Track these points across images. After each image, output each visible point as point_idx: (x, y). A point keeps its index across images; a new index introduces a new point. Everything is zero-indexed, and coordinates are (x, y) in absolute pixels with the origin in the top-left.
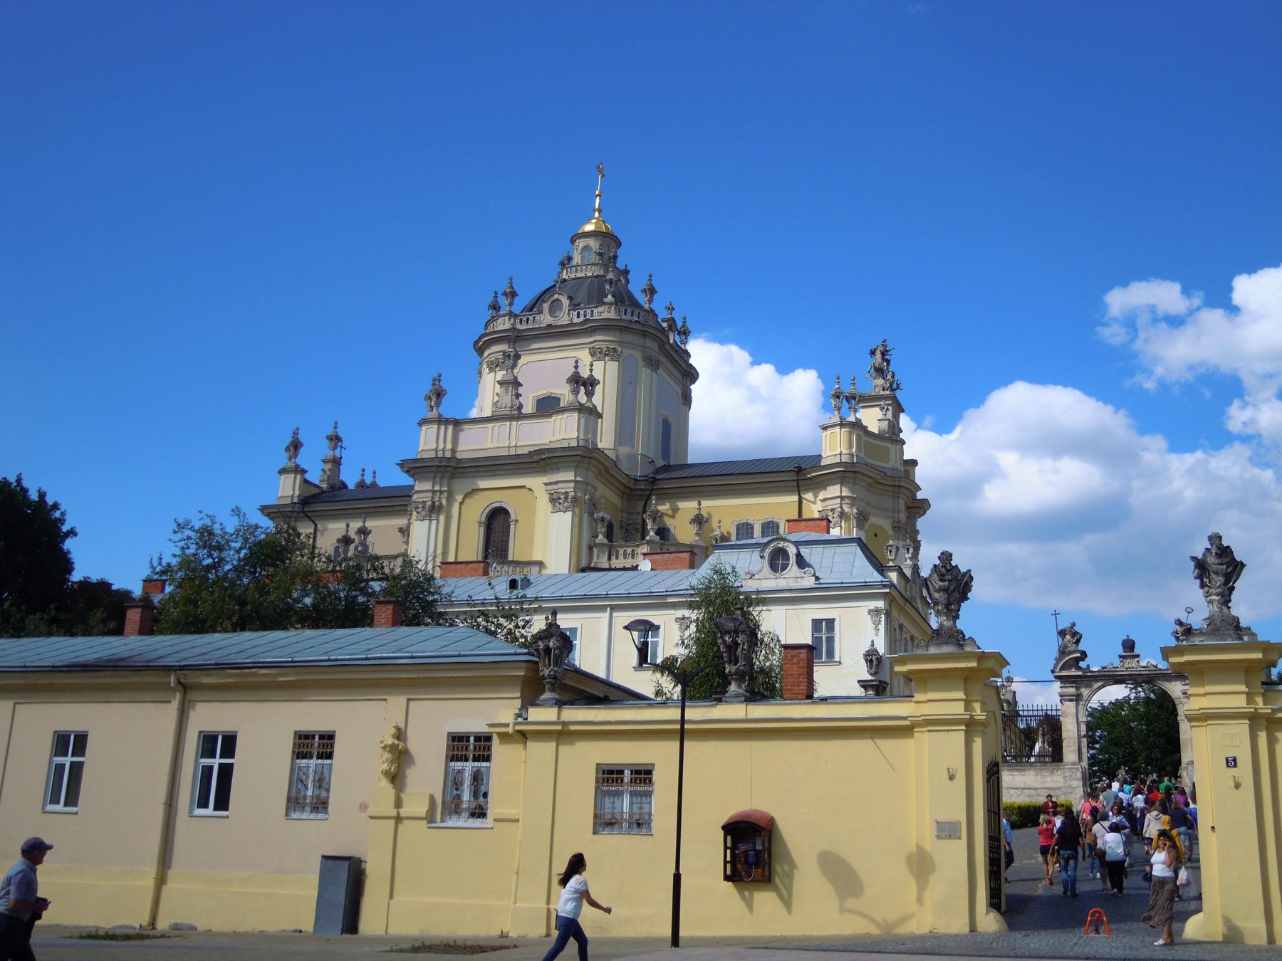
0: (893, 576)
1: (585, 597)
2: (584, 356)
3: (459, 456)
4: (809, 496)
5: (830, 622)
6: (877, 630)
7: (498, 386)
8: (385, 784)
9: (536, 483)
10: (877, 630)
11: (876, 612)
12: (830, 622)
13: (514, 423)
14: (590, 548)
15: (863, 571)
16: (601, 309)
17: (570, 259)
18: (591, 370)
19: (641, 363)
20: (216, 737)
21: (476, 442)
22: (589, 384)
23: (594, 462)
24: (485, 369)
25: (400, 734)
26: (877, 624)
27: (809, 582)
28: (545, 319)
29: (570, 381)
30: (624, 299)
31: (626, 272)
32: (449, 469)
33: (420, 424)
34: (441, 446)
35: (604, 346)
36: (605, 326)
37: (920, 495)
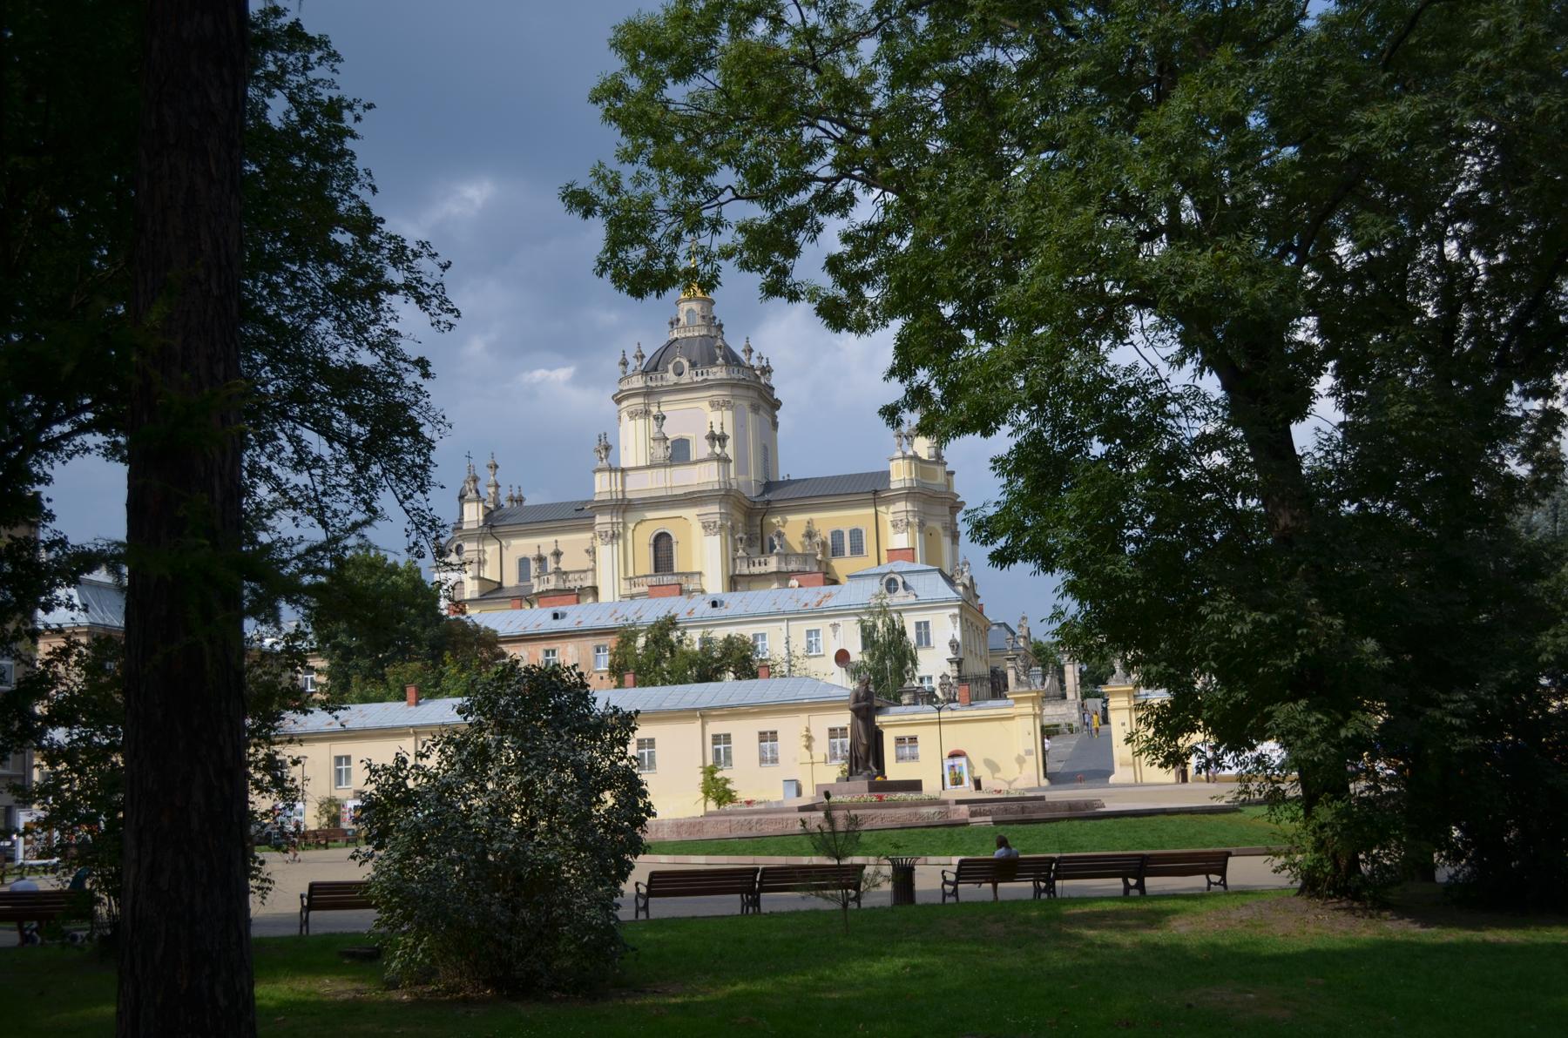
0: (961, 589)
1: (770, 614)
2: (705, 405)
3: (629, 496)
4: (882, 509)
5: (926, 623)
9: (690, 513)
11: (953, 616)
12: (926, 623)
15: (943, 590)
19: (748, 409)
21: (642, 485)
22: (722, 439)
24: (624, 415)
25: (808, 730)
27: (912, 599)
30: (731, 359)
31: (721, 326)
32: (623, 506)
35: (720, 399)
36: (720, 384)
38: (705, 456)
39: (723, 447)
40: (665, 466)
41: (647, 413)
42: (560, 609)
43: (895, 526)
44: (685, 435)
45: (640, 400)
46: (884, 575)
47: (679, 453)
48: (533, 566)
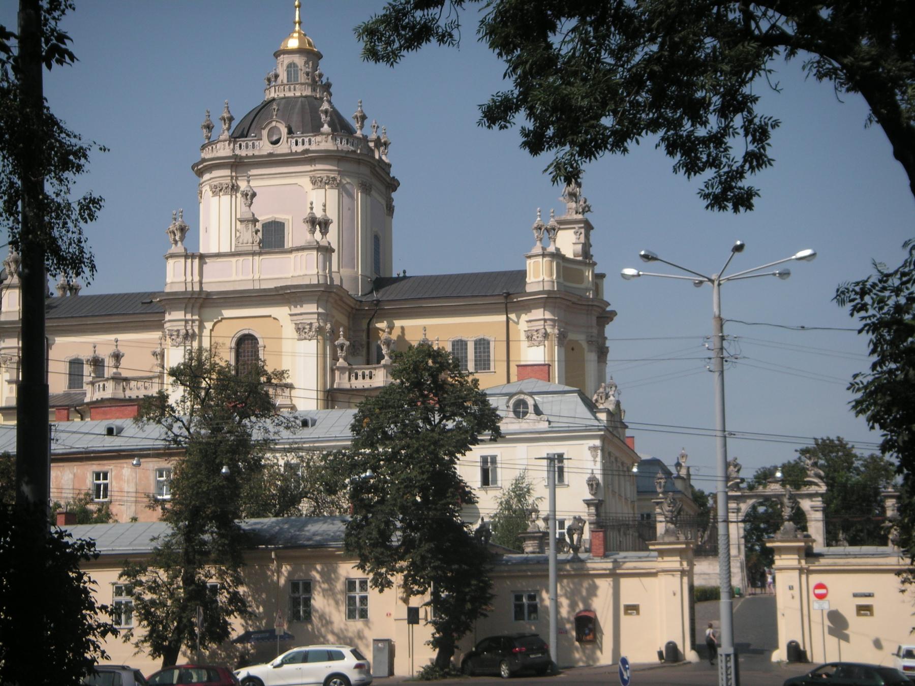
0: (603, 416)
2: (305, 182)
3: (206, 288)
4: (513, 316)
5: (560, 457)
6: (595, 461)
7: (238, 223)
8: (400, 603)
9: (281, 313)
10: (595, 461)
11: (593, 449)
13: (256, 258)
14: (333, 371)
16: (319, 138)
17: (276, 76)
18: (325, 210)
20: (298, 584)
21: (221, 276)
22: (324, 225)
23: (333, 295)
26: (595, 457)
27: (544, 426)
28: (264, 147)
29: (306, 221)
33: (167, 258)
34: (189, 279)
35: (324, 175)
37: (608, 309)
38: (302, 243)
39: (324, 232)
40: (254, 254)
41: (234, 189)
42: (116, 423)
43: (529, 338)
44: (280, 217)
45: (227, 172)
46: (511, 395)
47: (272, 238)
48: (87, 370)
